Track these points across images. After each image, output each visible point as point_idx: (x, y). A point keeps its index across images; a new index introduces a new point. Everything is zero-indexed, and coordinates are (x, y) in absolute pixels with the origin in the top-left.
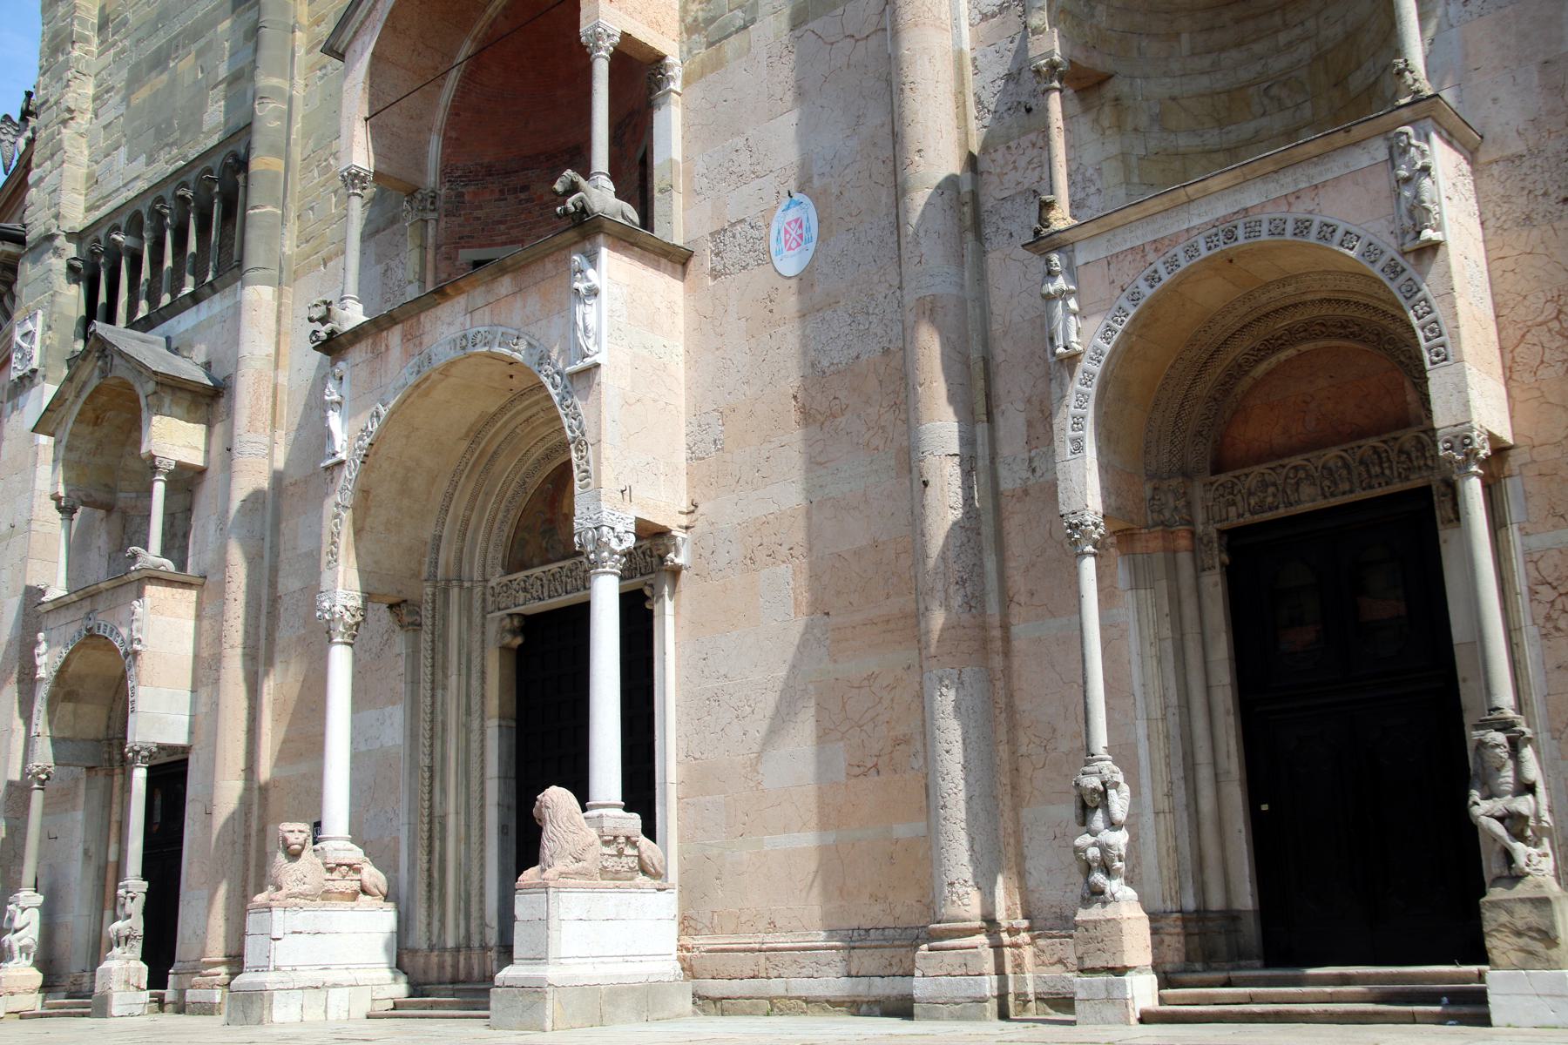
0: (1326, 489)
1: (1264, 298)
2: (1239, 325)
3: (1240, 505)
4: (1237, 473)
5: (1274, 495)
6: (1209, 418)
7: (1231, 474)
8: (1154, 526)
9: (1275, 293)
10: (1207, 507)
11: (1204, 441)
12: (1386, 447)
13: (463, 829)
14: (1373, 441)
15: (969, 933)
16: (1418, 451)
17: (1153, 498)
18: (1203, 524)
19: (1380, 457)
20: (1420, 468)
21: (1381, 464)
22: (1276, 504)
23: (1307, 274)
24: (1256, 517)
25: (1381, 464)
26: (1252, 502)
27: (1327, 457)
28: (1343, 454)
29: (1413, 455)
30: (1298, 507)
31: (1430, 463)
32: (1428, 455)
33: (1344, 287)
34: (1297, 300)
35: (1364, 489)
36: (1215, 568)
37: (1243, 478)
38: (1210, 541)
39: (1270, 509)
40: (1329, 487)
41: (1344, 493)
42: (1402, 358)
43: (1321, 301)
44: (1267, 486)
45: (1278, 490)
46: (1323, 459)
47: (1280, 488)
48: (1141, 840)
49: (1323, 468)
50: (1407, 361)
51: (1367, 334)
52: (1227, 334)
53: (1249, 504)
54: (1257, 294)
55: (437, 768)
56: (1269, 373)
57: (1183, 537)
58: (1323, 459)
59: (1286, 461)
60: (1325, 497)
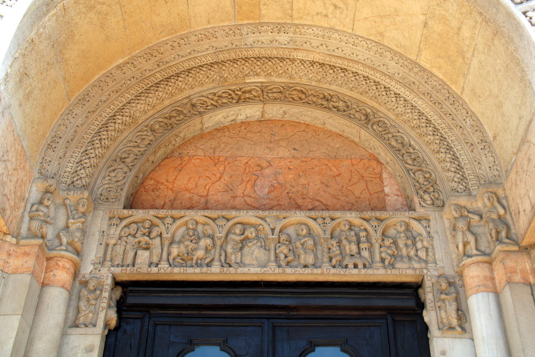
0: (282, 256)
1: (250, 39)
2: (210, 60)
3: (157, 251)
4: (162, 213)
5: (207, 250)
6: (138, 146)
7: (152, 212)
8: (27, 238)
9: (265, 38)
10: (107, 245)
11: (126, 169)
12: (365, 223)
14: (353, 217)
16: (408, 238)
17: (41, 203)
18: (94, 264)
19: (357, 235)
20: (410, 258)
21: (358, 243)
22: (208, 260)
23: (310, 26)
24: (176, 270)
25: (358, 243)
26: (175, 251)
27: (287, 220)
28: (311, 223)
29: (401, 243)
30: (240, 270)
31: (422, 254)
32: (419, 245)
33: (348, 51)
34: (286, 54)
35: (334, 267)
36: (95, 326)
37: (169, 220)
38: (99, 288)
39: (198, 265)
40: (286, 257)
41: (305, 266)
42: (394, 143)
43: (313, 63)
44: (199, 239)
45: (214, 245)
46: (284, 222)
47: (219, 243)
49: (280, 232)
50: (399, 146)
51: (352, 112)
52: (192, 64)
53: (169, 254)
54: (245, 31)
56: (220, 130)
57: (64, 267)
58: (284, 222)
59: (234, 213)
60: (279, 266)
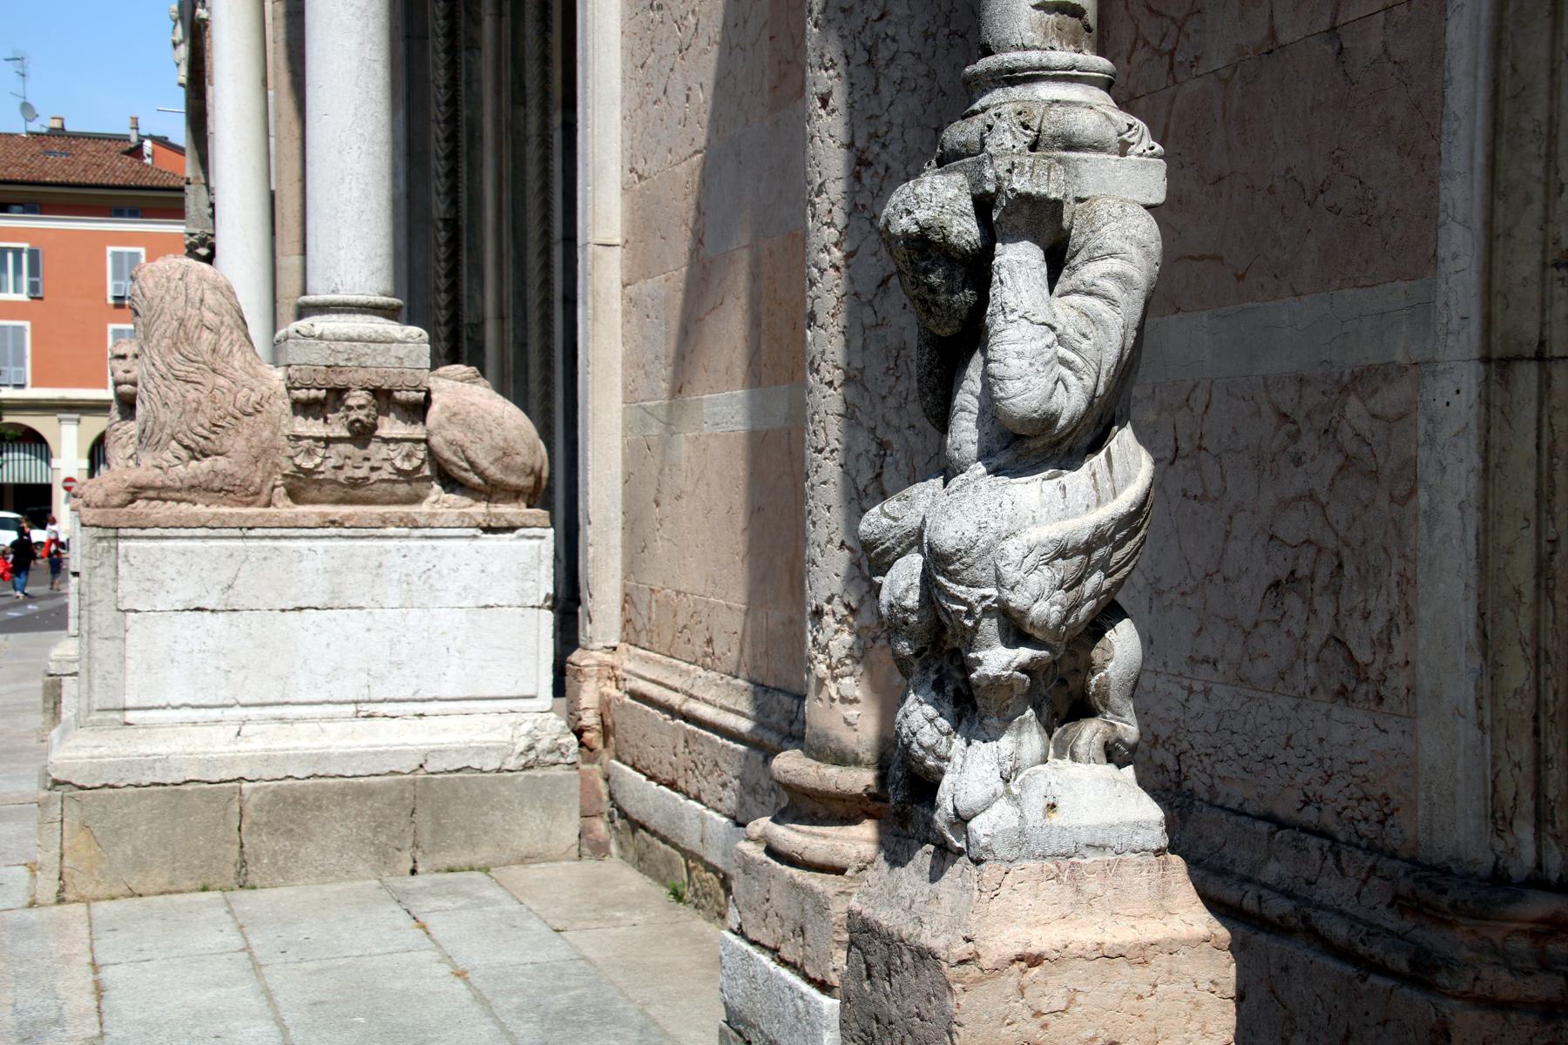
13: (511, 351)
15: (839, 808)
48: (1423, 498)
55: (464, 223)
